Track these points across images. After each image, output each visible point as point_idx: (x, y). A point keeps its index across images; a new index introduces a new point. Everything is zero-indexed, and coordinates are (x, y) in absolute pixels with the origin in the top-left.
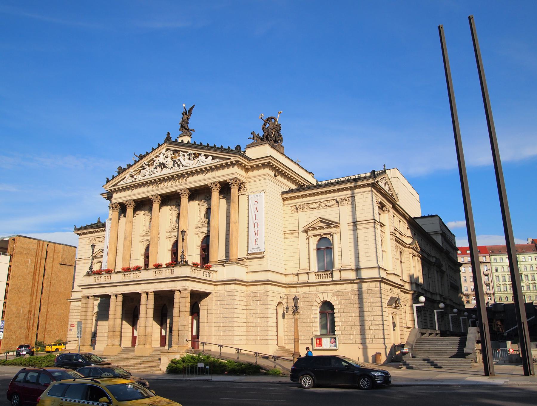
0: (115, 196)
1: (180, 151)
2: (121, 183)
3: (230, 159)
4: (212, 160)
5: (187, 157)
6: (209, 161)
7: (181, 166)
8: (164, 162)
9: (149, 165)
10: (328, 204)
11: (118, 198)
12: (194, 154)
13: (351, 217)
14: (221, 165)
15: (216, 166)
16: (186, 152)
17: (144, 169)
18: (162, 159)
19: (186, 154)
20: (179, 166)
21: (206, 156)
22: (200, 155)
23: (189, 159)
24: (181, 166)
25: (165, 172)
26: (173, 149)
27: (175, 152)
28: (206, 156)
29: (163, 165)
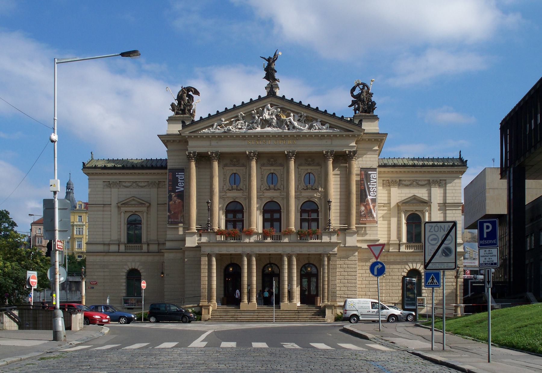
0: (191, 143)
1: (289, 110)
2: (206, 131)
3: (353, 131)
4: (330, 127)
5: (297, 118)
6: (325, 130)
7: (291, 127)
8: (267, 117)
9: (243, 118)
10: (420, 183)
11: (195, 146)
12: (306, 117)
13: (442, 198)
14: (341, 136)
15: (335, 136)
16: (297, 113)
17: (239, 120)
18: (266, 116)
19: (296, 115)
20: (288, 126)
21: (323, 123)
22: (316, 120)
23: (299, 120)
24: (291, 127)
25: (268, 129)
26: (281, 106)
27: (283, 110)
28: (323, 123)
29: (266, 123)
